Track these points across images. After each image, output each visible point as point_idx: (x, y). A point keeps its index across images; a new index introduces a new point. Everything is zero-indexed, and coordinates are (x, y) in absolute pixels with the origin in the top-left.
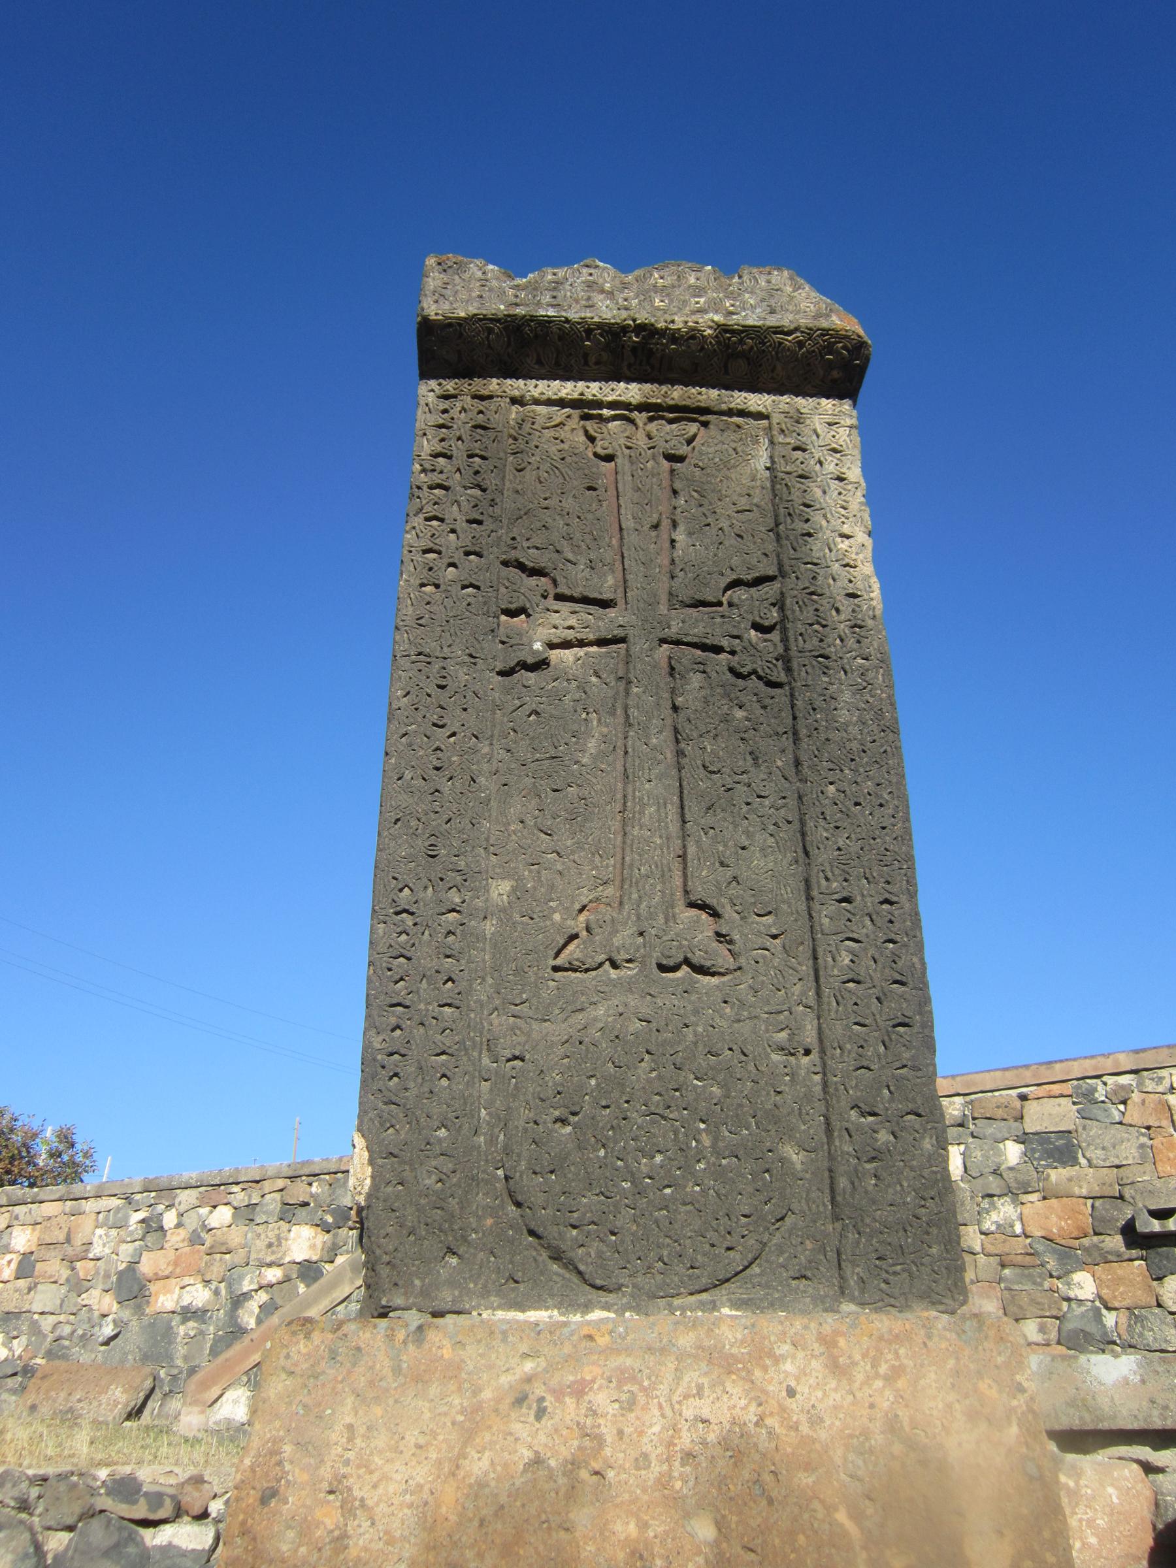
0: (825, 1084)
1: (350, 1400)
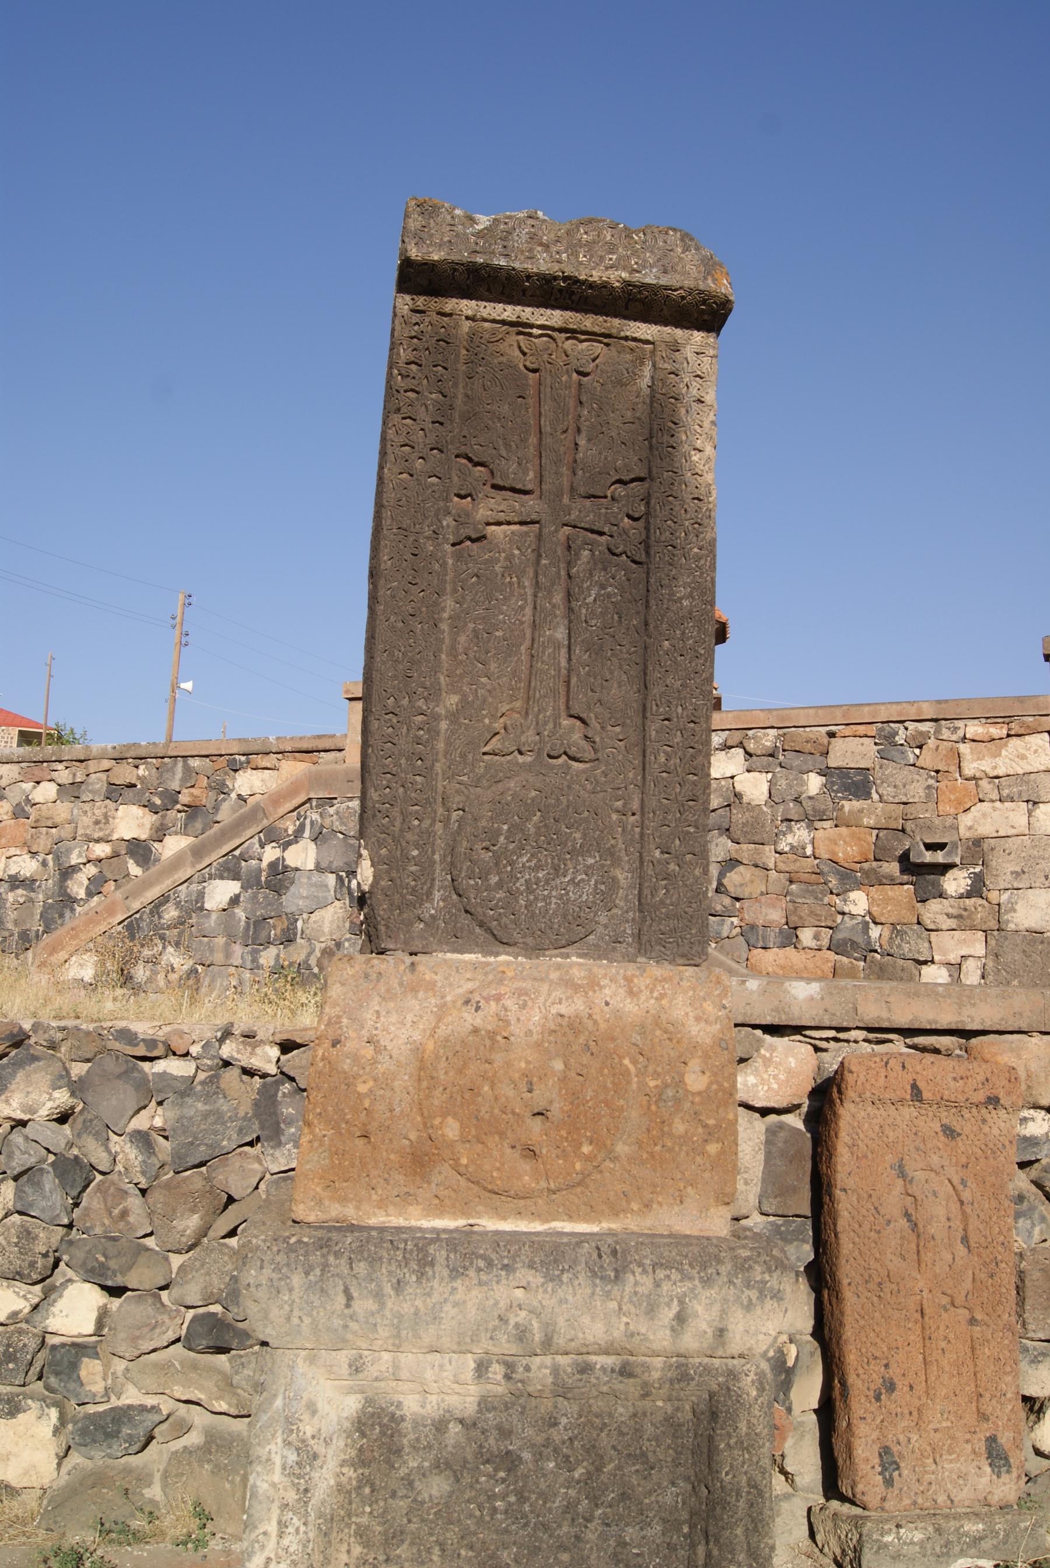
0: (642, 835)
1: (377, 999)
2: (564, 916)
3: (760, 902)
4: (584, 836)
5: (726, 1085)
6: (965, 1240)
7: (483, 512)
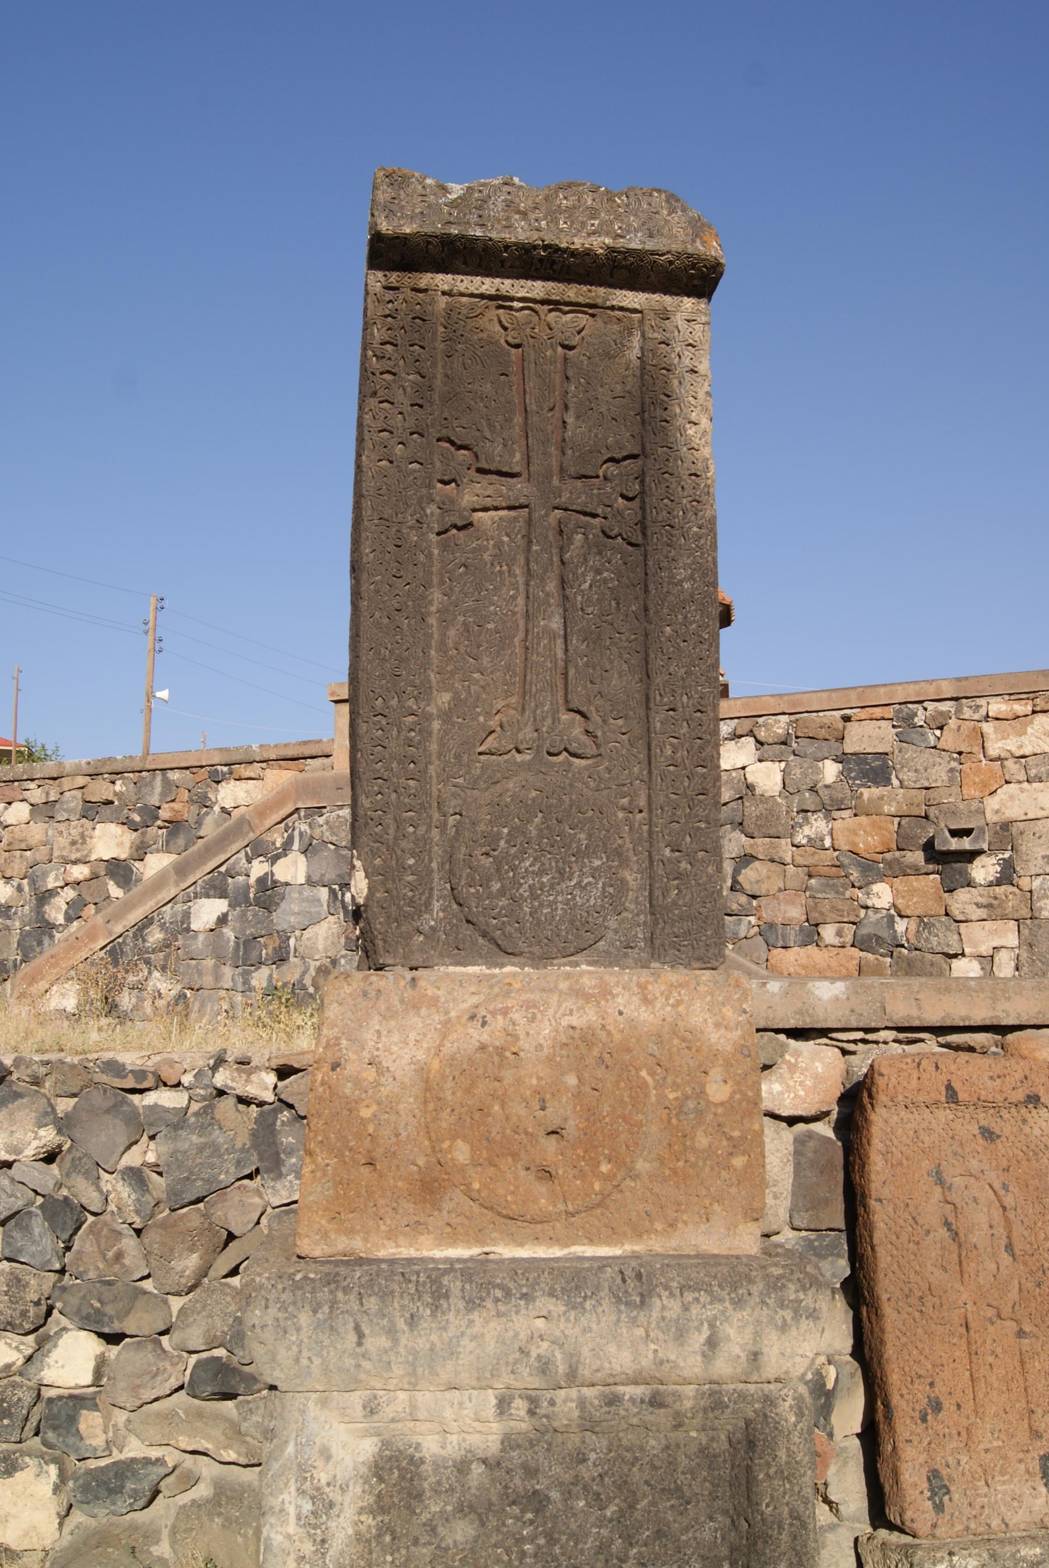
0: (650, 833)
1: (377, 1018)
2: (572, 922)
3: (778, 899)
4: (590, 836)
5: (750, 1094)
6: (1009, 1248)
7: (468, 498)
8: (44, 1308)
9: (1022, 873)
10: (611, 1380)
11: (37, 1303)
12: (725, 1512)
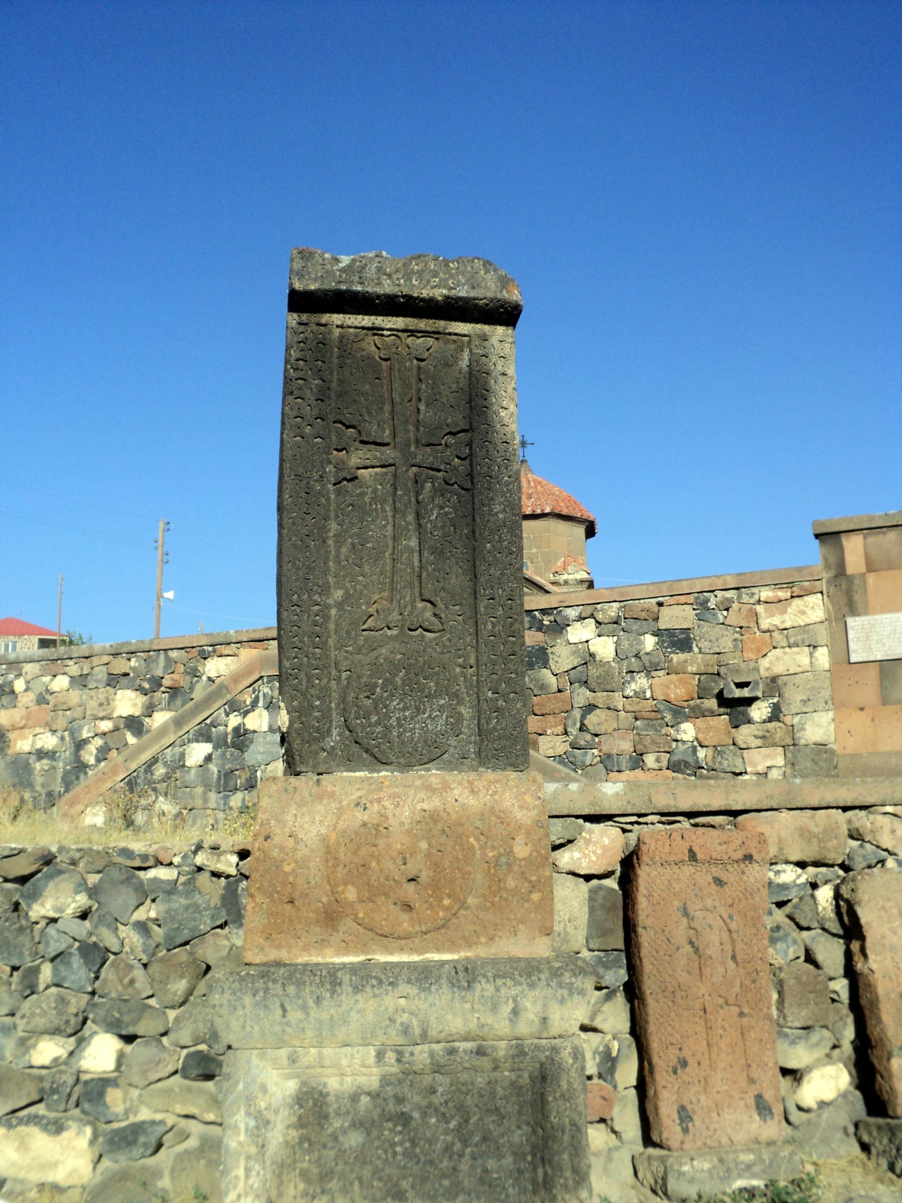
0: (478, 681)
1: (294, 806)
2: (426, 741)
4: (437, 684)
6: (734, 958)
7: (355, 460)
8: (81, 1018)
9: (786, 712)
10: (451, 1039)
11: (77, 1015)
12: (528, 1124)
